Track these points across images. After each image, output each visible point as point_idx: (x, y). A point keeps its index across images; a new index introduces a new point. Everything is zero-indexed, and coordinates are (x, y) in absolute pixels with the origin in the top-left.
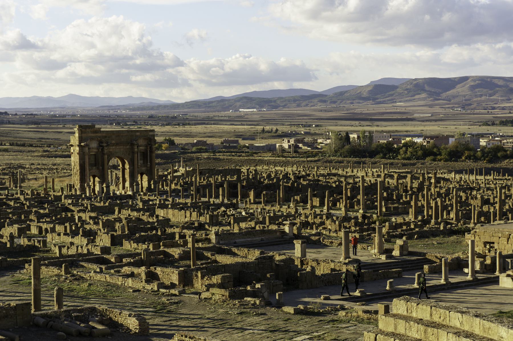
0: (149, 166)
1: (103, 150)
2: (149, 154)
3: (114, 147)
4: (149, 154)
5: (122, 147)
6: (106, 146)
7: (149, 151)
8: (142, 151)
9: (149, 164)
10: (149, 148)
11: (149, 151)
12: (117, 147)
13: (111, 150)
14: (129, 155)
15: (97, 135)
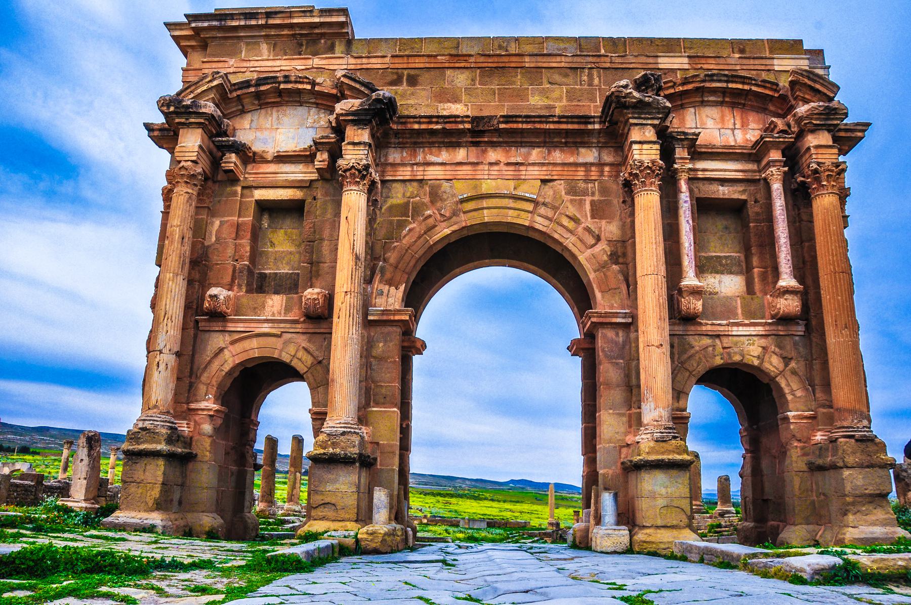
0: (790, 305)
1: (336, 153)
2: (779, 204)
3: (461, 154)
4: (779, 204)
5: (535, 154)
6: (359, 118)
7: (777, 187)
8: (724, 192)
9: (787, 280)
10: (775, 155)
11: (777, 187)
12: (493, 155)
13: (433, 173)
14: (598, 211)
15: (317, 61)
